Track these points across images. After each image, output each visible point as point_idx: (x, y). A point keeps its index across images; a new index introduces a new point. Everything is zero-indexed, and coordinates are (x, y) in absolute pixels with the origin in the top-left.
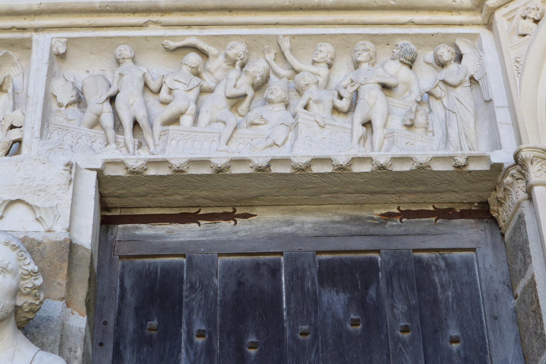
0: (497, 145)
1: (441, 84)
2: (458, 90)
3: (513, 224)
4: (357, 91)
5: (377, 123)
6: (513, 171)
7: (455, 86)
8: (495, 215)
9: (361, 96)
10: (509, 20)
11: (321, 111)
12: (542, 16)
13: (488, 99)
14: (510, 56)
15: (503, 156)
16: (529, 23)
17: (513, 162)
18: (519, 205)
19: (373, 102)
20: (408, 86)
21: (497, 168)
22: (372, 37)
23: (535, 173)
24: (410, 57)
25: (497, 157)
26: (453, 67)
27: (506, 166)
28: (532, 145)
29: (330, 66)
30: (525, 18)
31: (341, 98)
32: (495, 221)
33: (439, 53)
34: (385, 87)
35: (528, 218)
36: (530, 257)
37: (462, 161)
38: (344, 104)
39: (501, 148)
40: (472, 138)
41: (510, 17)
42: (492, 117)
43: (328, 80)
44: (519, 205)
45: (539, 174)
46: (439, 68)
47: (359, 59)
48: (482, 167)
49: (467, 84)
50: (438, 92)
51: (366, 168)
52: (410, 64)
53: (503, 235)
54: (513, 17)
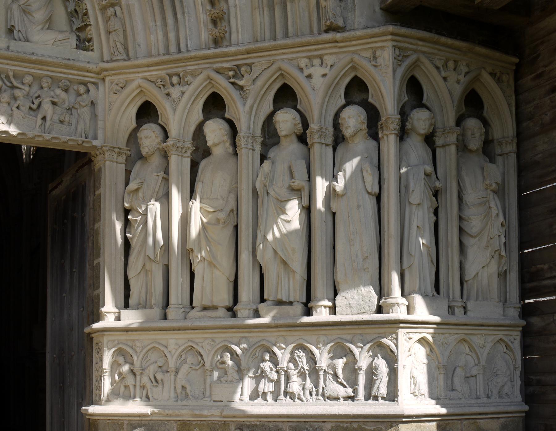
0: (95, 138)
2: (85, 108)
4: (41, 102)
5: (48, 118)
7: (84, 107)
9: (42, 105)
11: (25, 109)
19: (47, 107)
20: (64, 101)
22: (51, 77)
24: (66, 88)
26: (85, 96)
29: (30, 86)
30: (117, 85)
31: (33, 103)
34: (54, 103)
35: (103, 170)
37: (80, 142)
38: (34, 107)
39: (97, 139)
43: (28, 93)
47: (44, 86)
48: (89, 145)
49: (89, 106)
50: (77, 106)
51: (41, 139)
52: (66, 91)
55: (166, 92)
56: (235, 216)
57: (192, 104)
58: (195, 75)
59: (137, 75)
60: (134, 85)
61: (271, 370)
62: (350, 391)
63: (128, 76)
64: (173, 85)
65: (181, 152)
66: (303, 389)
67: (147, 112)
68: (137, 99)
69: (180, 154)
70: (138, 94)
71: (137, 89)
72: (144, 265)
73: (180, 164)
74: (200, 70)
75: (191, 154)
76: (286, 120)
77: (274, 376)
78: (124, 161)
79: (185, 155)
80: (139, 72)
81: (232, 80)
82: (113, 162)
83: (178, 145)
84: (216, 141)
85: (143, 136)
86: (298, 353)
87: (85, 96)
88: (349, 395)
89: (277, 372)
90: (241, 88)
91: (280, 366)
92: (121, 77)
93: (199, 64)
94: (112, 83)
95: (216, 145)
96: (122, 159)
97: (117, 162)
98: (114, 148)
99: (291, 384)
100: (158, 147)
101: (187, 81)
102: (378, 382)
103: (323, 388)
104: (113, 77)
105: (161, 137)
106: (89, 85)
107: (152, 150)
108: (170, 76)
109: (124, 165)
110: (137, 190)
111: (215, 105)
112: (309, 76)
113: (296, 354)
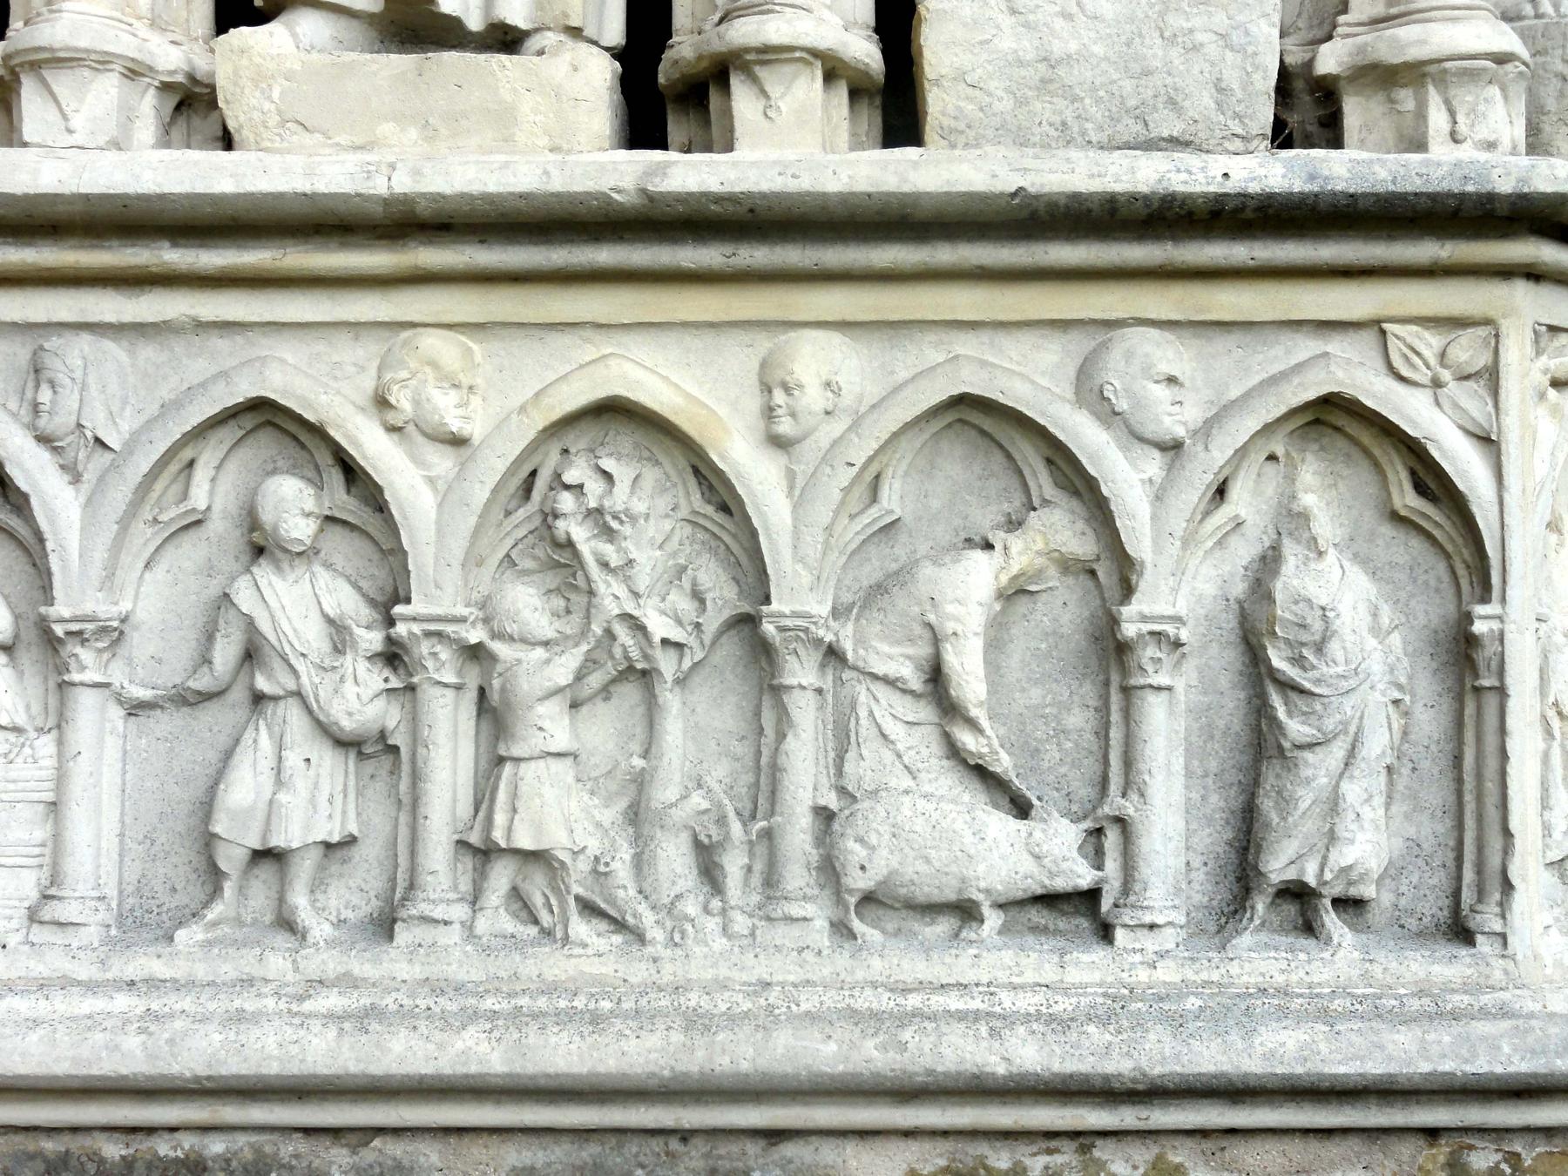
61: (339, 634)
62: (1055, 851)
66: (636, 816)
77: (360, 697)
86: (594, 487)
88: (1061, 884)
89: (393, 656)
91: (417, 607)
99: (528, 771)
102: (1320, 768)
103: (825, 816)
113: (566, 501)
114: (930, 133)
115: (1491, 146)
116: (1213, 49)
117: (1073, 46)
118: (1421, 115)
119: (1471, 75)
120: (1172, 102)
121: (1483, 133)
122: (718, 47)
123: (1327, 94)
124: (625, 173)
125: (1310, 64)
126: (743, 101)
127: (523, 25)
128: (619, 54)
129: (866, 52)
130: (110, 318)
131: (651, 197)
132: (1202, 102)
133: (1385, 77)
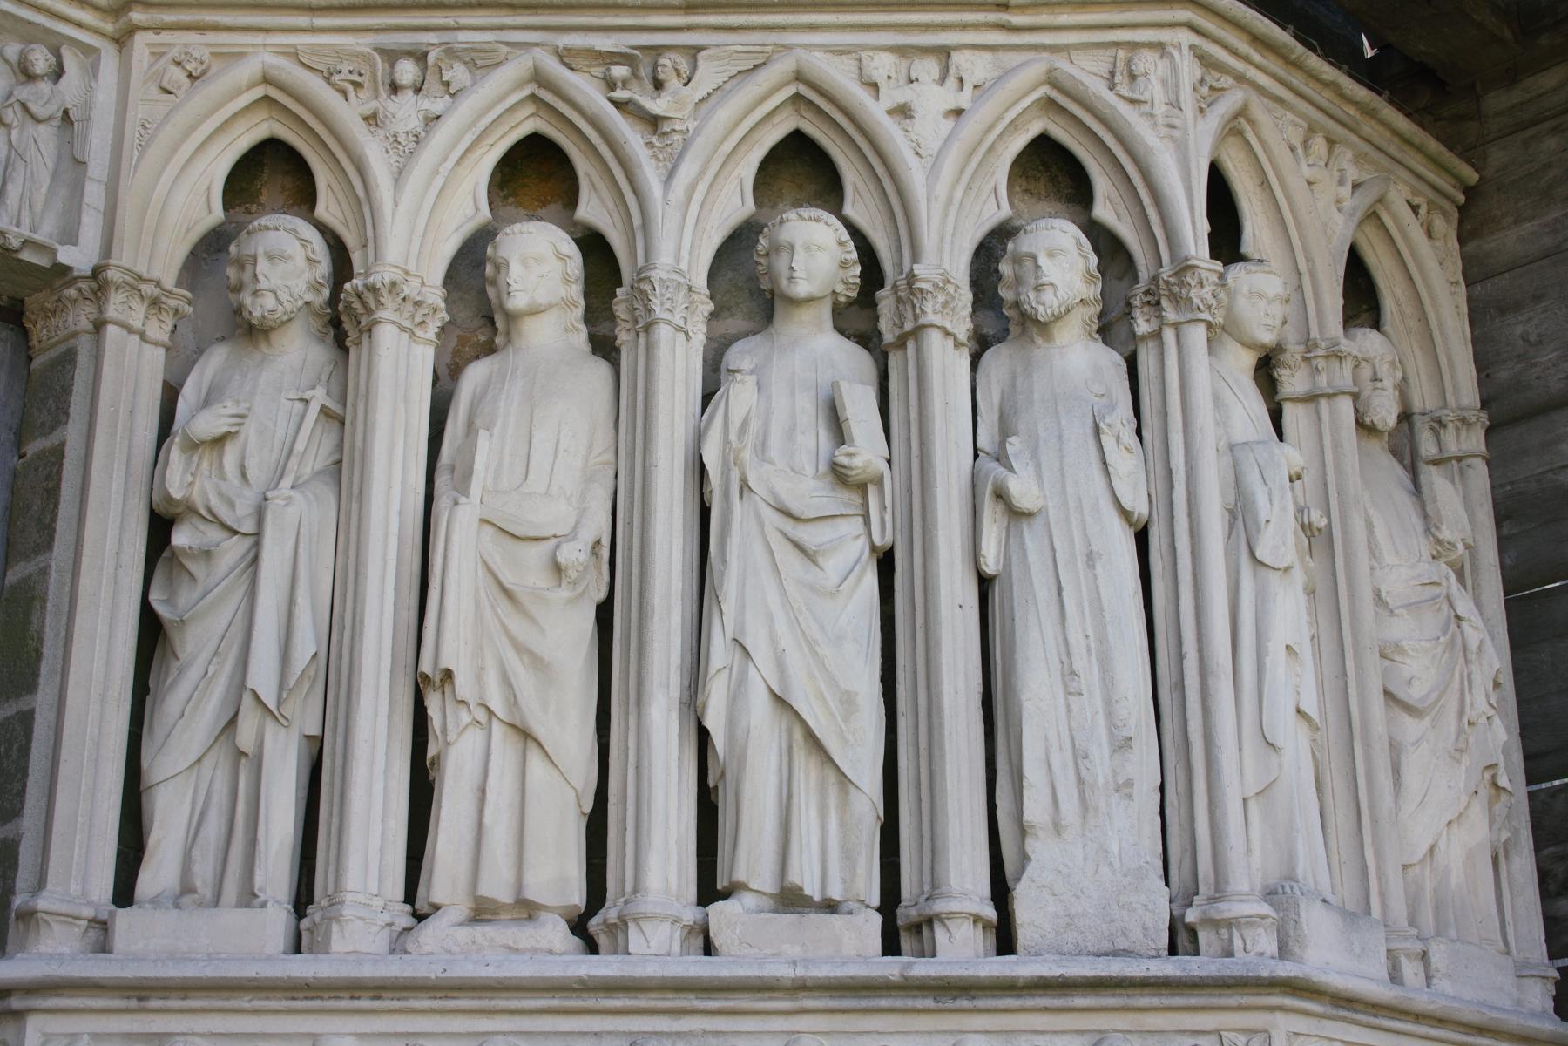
0: (70, 236)
1: (17, 107)
2: (42, 128)
3: (53, 353)
6: (84, 286)
7: (38, 121)
8: (28, 325)
10: (153, 54)
12: (204, 73)
13: (80, 158)
14: (137, 112)
15: (79, 258)
16: (178, 75)
17: (89, 273)
18: (75, 335)
21: (62, 271)
23: (115, 306)
25: (66, 256)
27: (76, 273)
28: (125, 263)
30: (179, 64)
32: (25, 334)
33: (31, 57)
35: (83, 359)
36: (67, 414)
37: (15, 243)
39: (75, 243)
40: (38, 208)
41: (156, 50)
42: (78, 189)
44: (75, 335)
45: (120, 308)
46: (22, 78)
49: (57, 122)
53: (30, 359)
54: (162, 54)
55: (367, 109)
56: (605, 568)
57: (458, 163)
58: (481, 62)
59: (260, 39)
60: (247, 70)
63: (224, 37)
64: (395, 88)
65: (412, 317)
67: (273, 172)
68: (240, 126)
69: (407, 324)
70: (248, 108)
71: (252, 86)
72: (232, 722)
73: (401, 360)
74: (505, 49)
75: (438, 335)
76: (814, 249)
78: (165, 338)
79: (419, 333)
80: (267, 30)
81: (620, 94)
82: (130, 330)
83: (407, 291)
84: (542, 298)
85: (260, 251)
87: (44, 87)
90: (654, 122)
92: (193, 37)
93: (502, 28)
94: (158, 56)
95: (535, 311)
96: (159, 330)
97: (143, 336)
98: (140, 278)
100: (309, 297)
101: (448, 84)
104: (165, 37)
105: (324, 267)
106: (65, 51)
107: (288, 307)
108: (392, 56)
109: (162, 351)
110: (220, 441)
111: (535, 171)
112: (903, 112)
114: (1020, 948)
115: (1262, 954)
116: (1140, 912)
117: (1080, 910)
118: (1231, 940)
119: (1251, 925)
120: (1124, 934)
121: (1259, 949)
122: (929, 912)
123: (1192, 932)
124: (891, 968)
125: (1183, 916)
126: (940, 933)
127: (838, 898)
128: (879, 910)
129: (990, 913)
130: (665, 1029)
131: (906, 978)
132: (1136, 934)
133: (1215, 924)
